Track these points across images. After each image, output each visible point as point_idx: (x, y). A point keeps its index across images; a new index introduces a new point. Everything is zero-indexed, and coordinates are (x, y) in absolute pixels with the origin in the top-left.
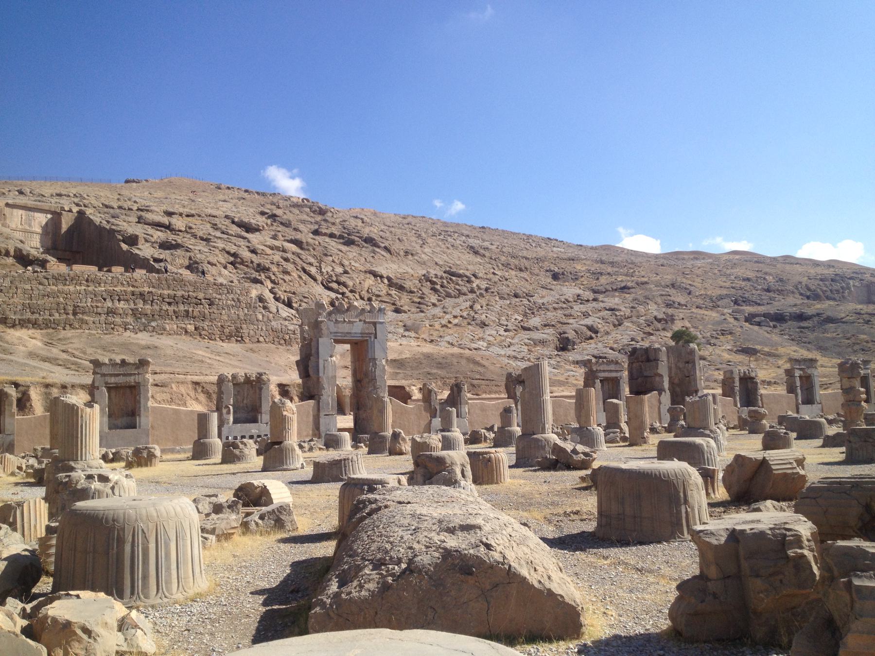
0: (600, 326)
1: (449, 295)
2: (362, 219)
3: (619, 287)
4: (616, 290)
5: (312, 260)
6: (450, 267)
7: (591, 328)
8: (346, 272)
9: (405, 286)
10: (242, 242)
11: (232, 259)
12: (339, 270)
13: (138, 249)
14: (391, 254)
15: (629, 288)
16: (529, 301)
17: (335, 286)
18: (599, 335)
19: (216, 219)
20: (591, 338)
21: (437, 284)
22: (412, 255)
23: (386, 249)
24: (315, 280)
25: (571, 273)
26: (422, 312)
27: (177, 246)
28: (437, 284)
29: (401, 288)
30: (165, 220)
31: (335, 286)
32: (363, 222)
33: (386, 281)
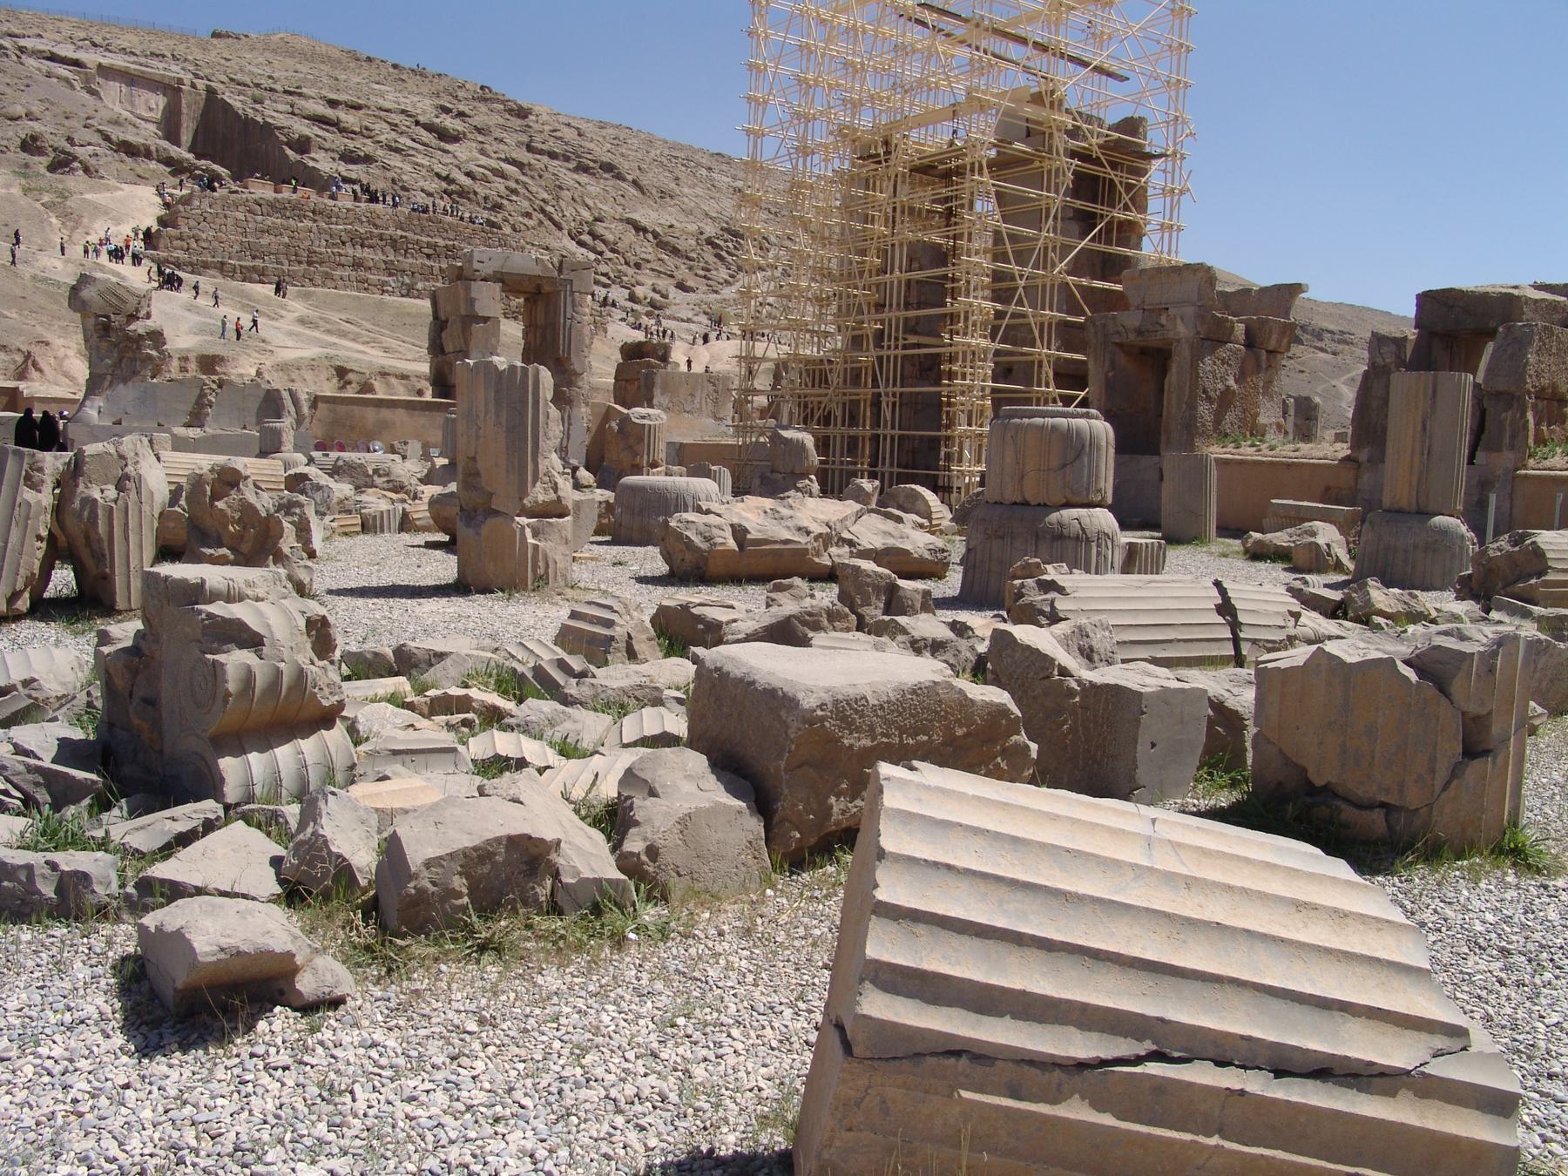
2: (578, 129)
5: (545, 196)
8: (597, 220)
10: (447, 159)
11: (444, 185)
12: (586, 214)
13: (313, 159)
17: (586, 238)
19: (393, 115)
22: (671, 197)
23: (635, 183)
24: (560, 229)
26: (716, 292)
27: (368, 159)
29: (675, 251)
30: (329, 112)
31: (586, 238)
33: (650, 237)
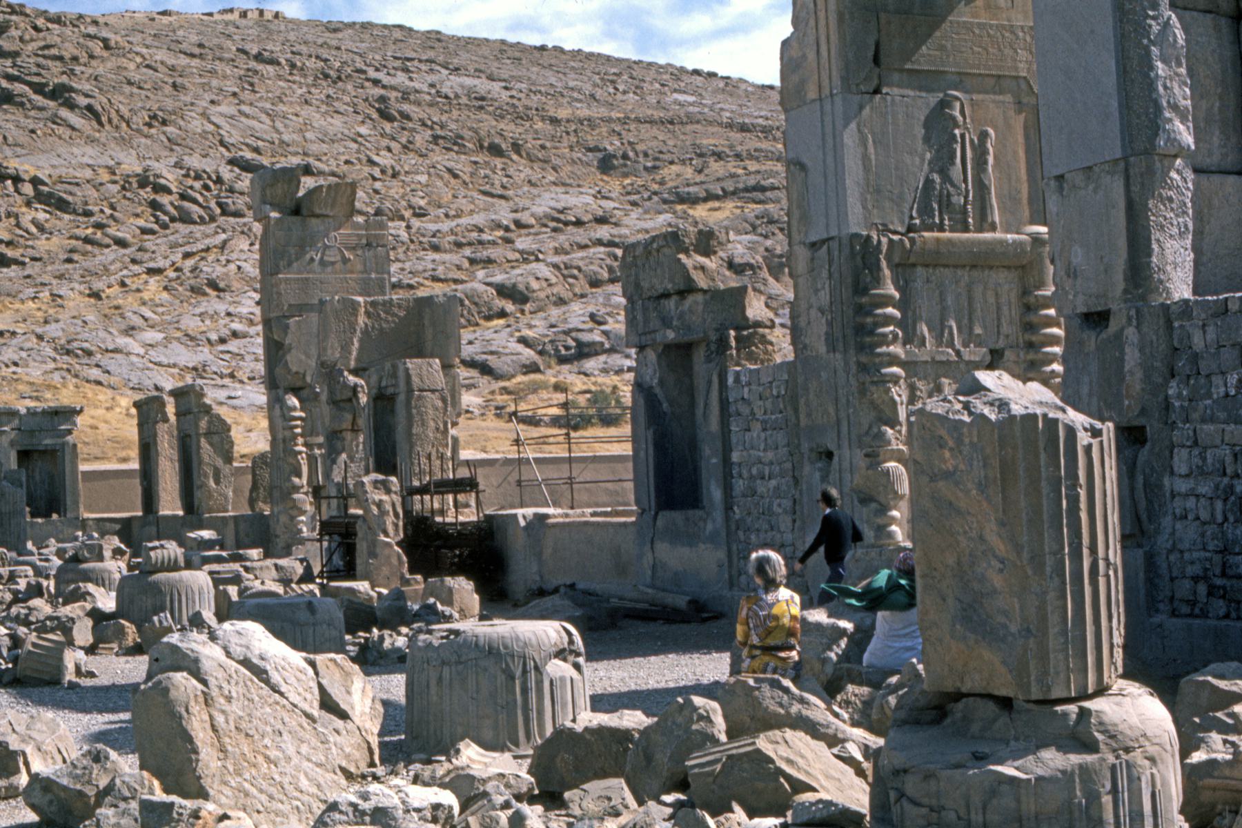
0: (535, 285)
1: (185, 218)
3: (741, 186)
4: (734, 193)
6: (256, 150)
7: (503, 291)
9: (70, 199)
14: (100, 124)
15: (763, 189)
16: (408, 227)
18: (528, 307)
20: (502, 314)
21: (169, 192)
25: (646, 155)
28: (169, 192)
32: (107, 47)
33: (28, 189)
